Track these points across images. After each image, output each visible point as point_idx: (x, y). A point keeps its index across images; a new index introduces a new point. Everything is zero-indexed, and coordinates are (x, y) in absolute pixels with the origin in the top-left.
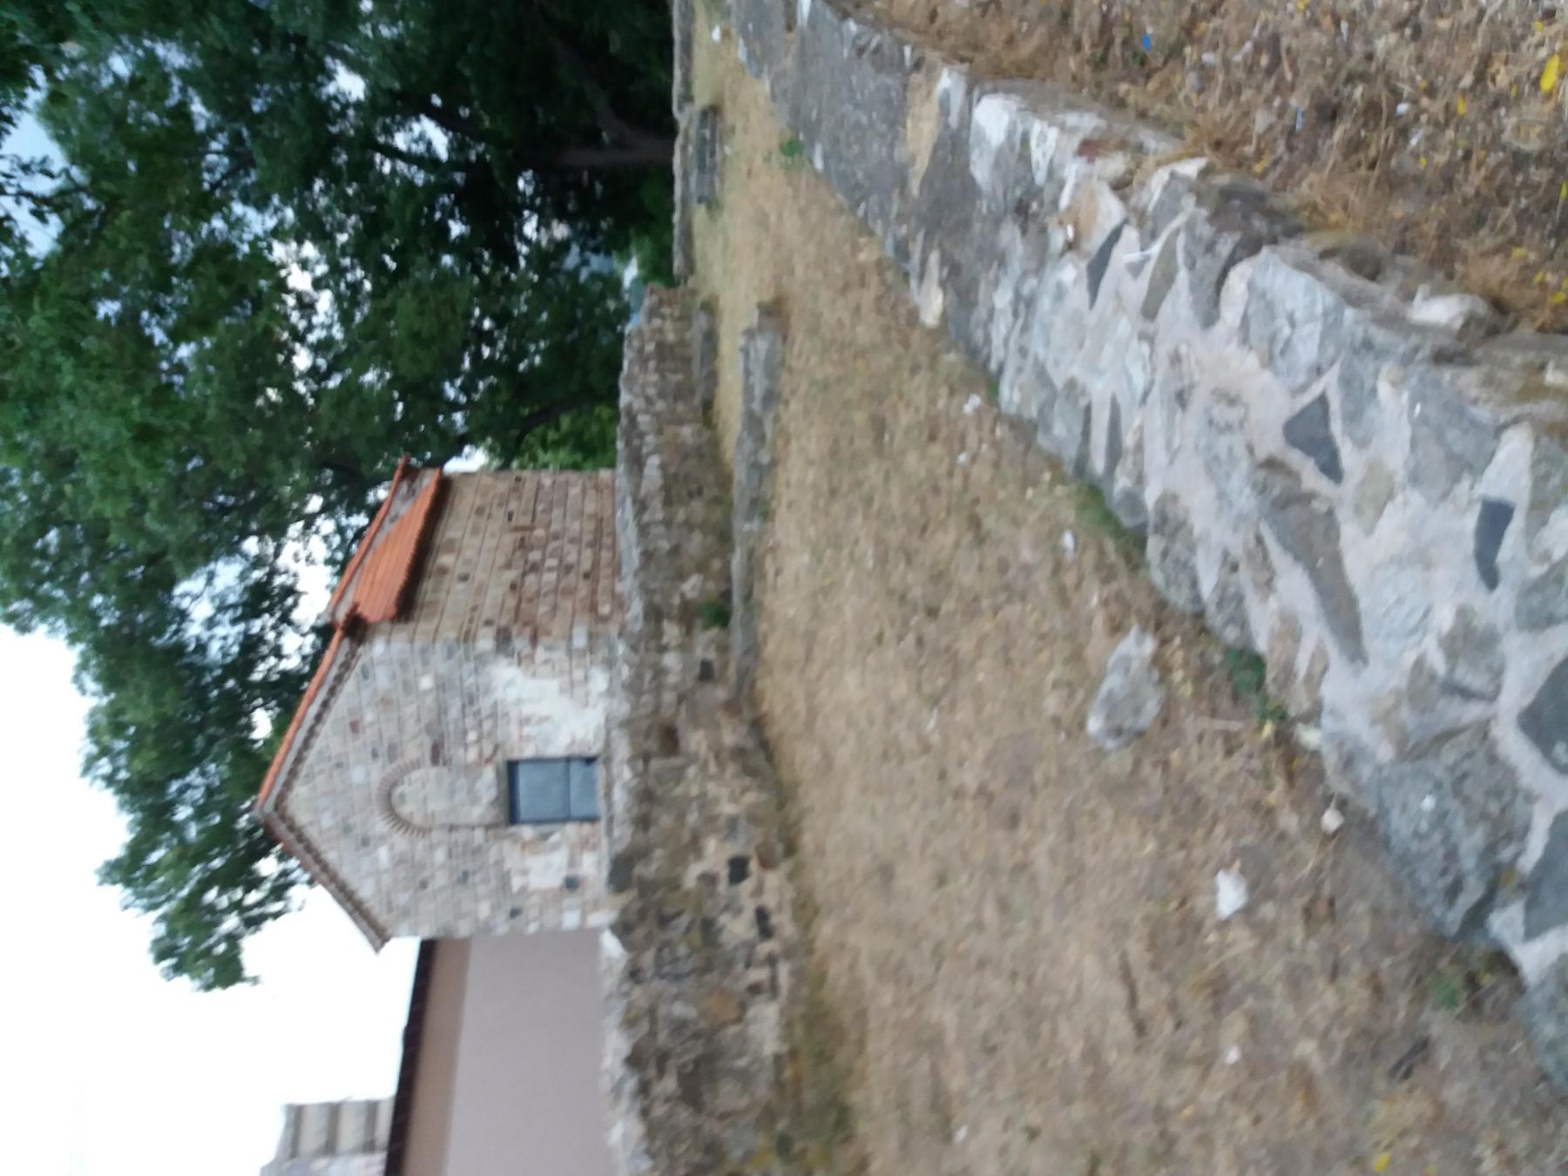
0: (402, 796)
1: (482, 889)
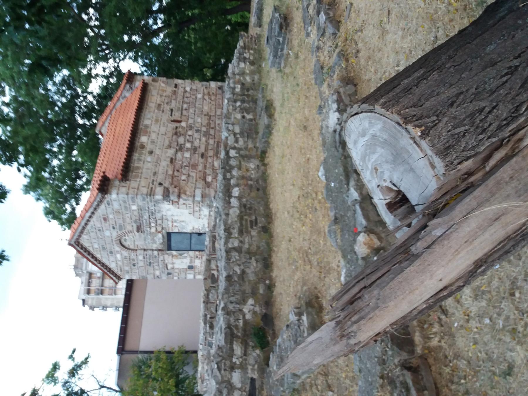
0: (125, 240)
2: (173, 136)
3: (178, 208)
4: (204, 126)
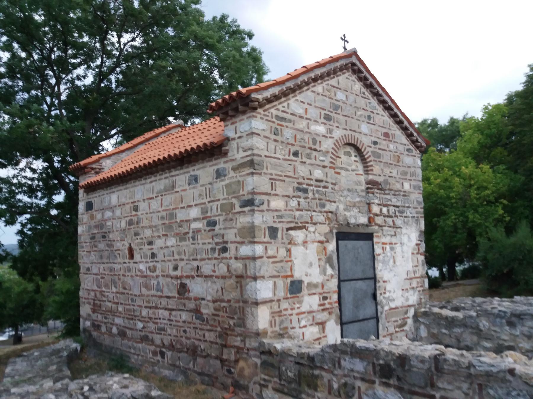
1: (293, 203)
3: (413, 254)
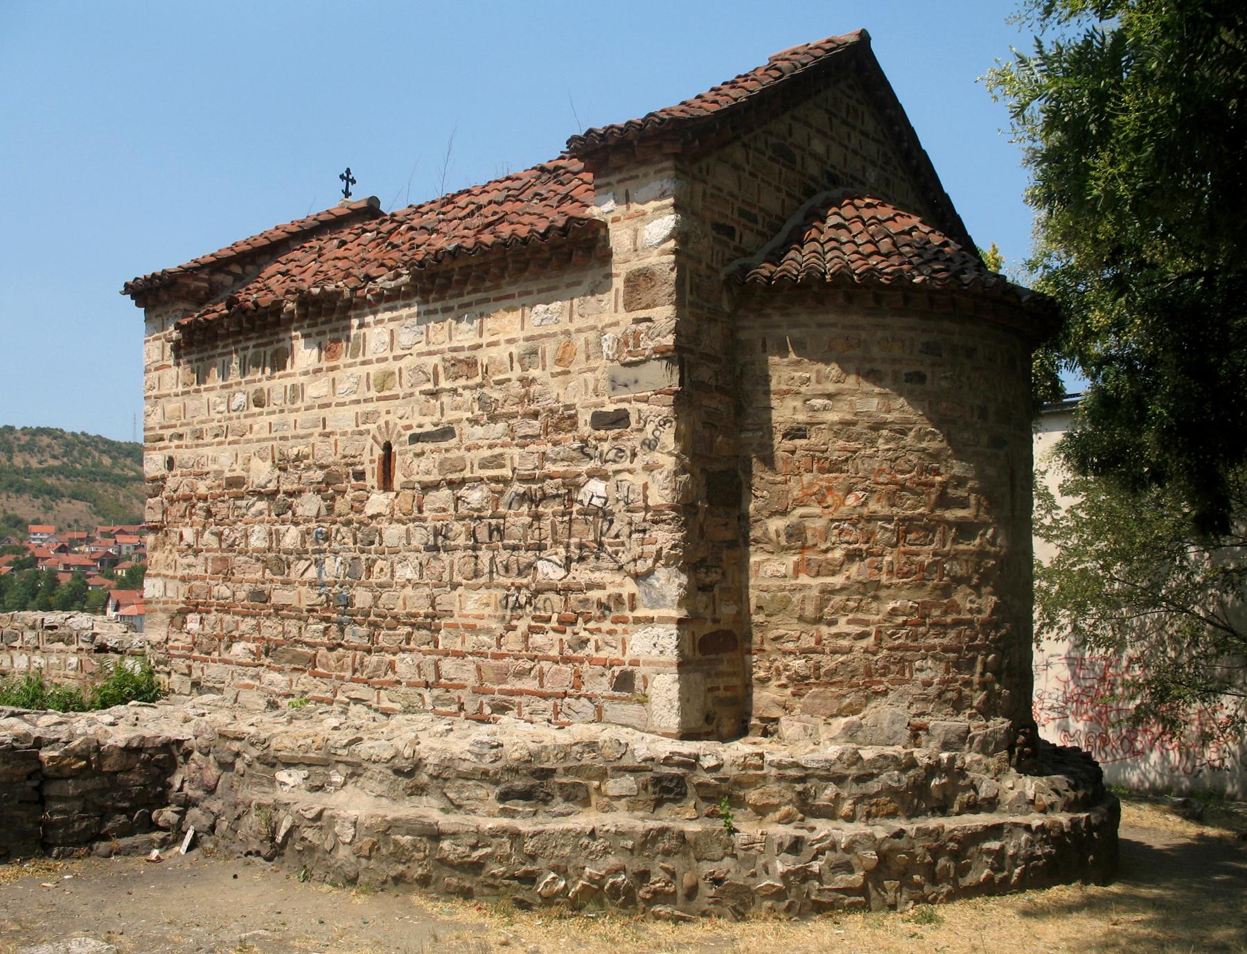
2: (322, 467)
4: (376, 599)
